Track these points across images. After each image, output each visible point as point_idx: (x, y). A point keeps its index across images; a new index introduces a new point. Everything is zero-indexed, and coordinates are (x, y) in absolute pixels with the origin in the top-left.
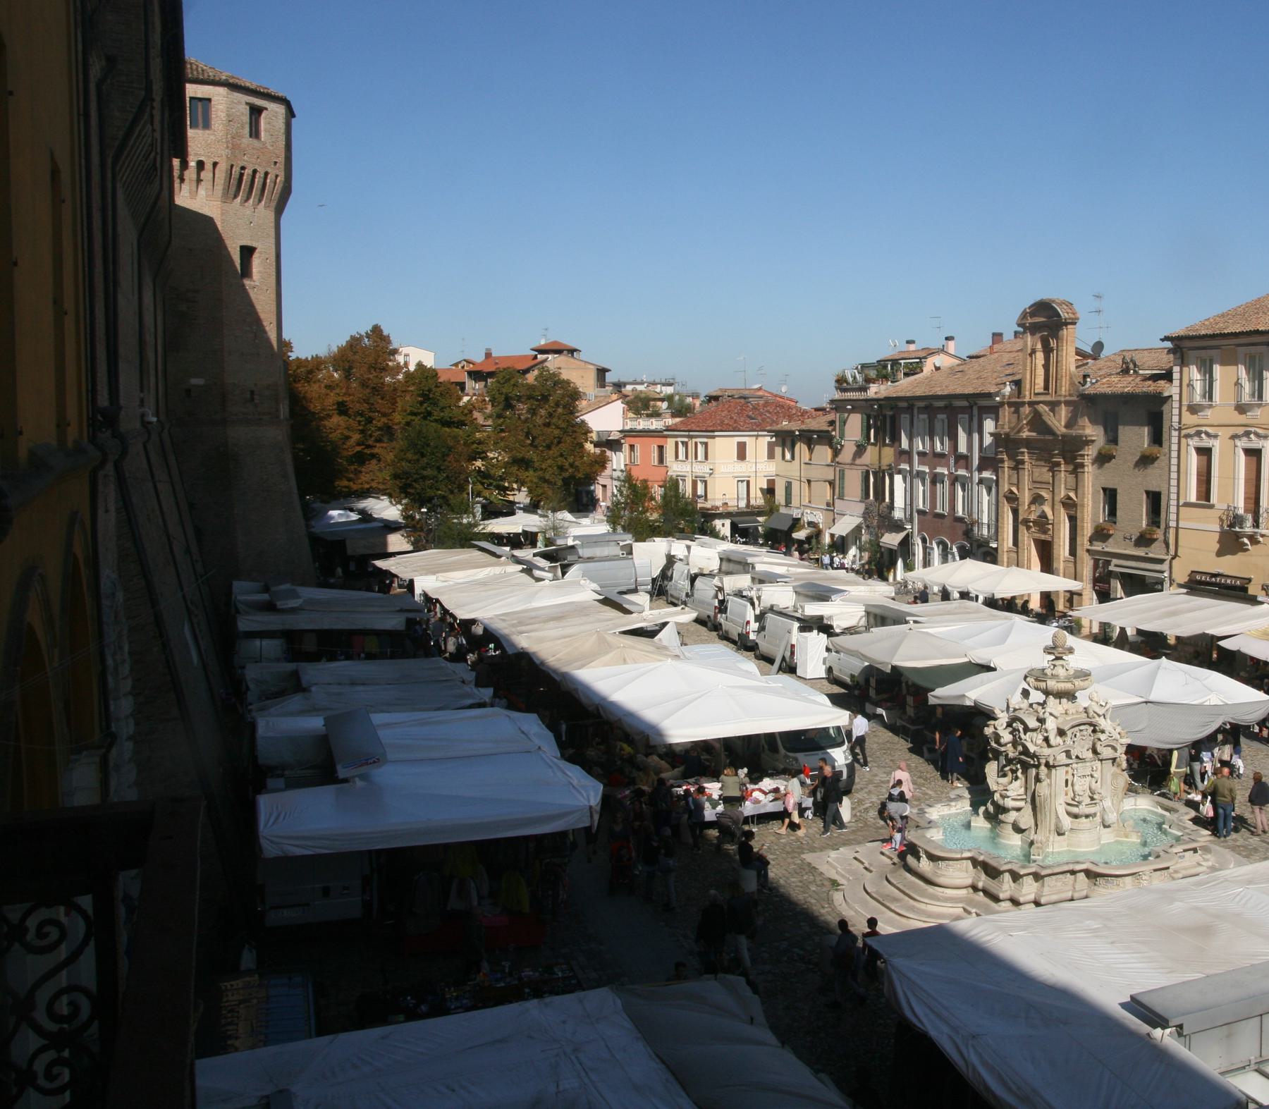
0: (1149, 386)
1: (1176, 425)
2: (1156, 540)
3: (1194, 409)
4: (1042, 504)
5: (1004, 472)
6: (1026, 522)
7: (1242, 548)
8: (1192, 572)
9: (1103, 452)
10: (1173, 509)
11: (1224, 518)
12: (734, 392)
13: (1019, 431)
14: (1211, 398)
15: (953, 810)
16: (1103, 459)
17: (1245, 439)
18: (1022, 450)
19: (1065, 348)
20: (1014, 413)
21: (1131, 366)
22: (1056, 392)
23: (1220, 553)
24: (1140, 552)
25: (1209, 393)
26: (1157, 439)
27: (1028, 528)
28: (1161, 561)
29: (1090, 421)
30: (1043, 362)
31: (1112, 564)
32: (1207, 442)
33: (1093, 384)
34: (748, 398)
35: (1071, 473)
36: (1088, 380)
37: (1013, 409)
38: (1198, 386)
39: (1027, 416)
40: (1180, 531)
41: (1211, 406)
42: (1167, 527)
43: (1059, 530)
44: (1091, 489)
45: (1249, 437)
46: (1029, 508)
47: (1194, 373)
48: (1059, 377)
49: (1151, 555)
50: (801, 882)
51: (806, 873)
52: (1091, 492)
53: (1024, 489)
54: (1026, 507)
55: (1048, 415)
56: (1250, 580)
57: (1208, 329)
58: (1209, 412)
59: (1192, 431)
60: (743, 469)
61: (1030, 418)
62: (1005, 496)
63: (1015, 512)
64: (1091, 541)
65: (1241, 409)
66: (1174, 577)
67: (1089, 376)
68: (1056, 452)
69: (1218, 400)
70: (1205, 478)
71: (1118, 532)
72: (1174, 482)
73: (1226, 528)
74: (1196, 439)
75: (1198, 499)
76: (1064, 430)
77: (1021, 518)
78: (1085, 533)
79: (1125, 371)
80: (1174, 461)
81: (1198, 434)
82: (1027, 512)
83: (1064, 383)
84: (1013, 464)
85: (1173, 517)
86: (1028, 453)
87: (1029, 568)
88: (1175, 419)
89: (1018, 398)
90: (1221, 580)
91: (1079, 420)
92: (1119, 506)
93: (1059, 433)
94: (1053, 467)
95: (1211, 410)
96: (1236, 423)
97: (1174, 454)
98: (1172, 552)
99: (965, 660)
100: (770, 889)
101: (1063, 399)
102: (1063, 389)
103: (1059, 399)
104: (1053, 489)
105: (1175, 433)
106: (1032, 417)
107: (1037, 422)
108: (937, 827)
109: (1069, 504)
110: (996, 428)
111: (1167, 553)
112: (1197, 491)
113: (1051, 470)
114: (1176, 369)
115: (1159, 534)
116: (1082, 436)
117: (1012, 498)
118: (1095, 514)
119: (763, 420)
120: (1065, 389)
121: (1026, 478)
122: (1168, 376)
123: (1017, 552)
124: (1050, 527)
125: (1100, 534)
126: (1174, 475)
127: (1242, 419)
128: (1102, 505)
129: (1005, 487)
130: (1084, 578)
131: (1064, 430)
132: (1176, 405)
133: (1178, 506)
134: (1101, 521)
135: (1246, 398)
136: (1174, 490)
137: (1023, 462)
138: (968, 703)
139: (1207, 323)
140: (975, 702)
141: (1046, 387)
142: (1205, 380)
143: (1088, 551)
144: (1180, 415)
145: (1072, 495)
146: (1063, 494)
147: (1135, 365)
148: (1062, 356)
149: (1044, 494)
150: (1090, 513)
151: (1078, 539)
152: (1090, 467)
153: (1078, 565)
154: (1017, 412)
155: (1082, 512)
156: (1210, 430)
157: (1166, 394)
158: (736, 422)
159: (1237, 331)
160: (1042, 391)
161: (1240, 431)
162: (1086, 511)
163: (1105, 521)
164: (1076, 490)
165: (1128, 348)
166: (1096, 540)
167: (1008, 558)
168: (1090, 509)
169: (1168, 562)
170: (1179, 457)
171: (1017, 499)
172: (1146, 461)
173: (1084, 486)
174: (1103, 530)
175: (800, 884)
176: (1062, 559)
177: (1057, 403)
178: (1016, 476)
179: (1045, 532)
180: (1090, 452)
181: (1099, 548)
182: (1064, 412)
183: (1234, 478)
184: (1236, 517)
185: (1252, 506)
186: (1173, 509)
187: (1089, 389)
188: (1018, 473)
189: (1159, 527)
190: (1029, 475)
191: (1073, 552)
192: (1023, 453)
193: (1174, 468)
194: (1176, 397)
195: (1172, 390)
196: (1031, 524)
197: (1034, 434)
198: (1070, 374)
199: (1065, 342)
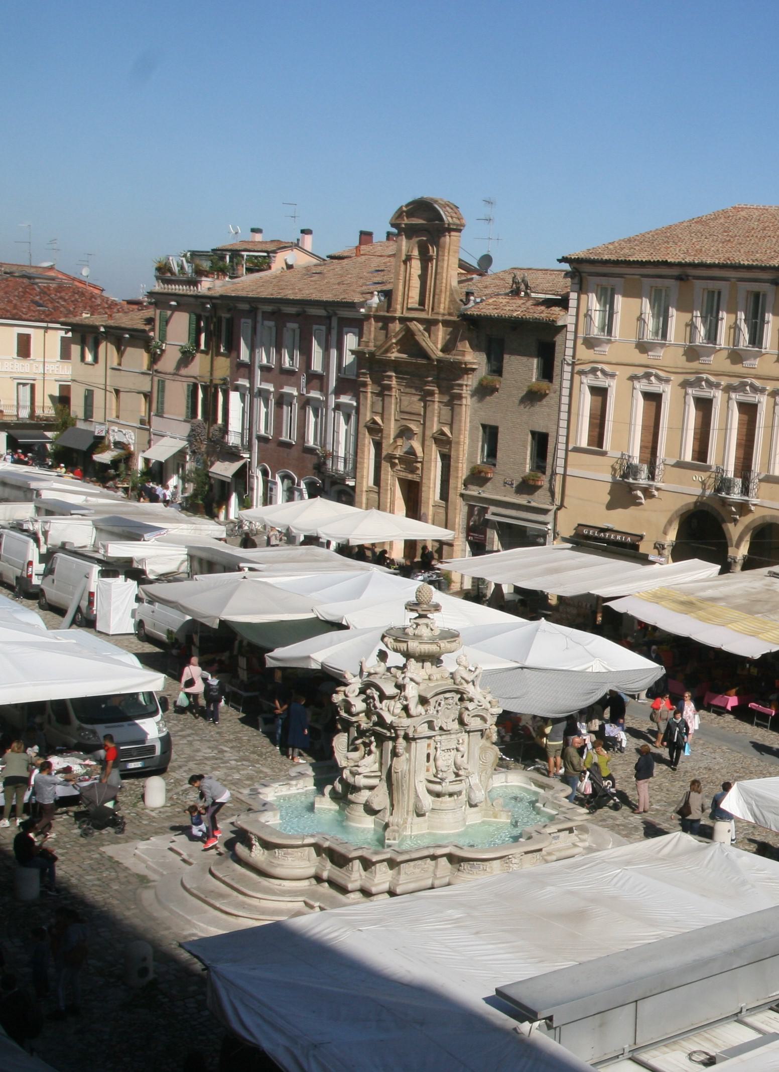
0: (542, 313)
1: (569, 359)
2: (540, 487)
3: (590, 343)
4: (410, 438)
5: (366, 398)
6: (390, 458)
7: (634, 502)
8: (579, 525)
9: (485, 383)
10: (561, 454)
11: (617, 467)
12: (14, 269)
13: (387, 351)
14: (610, 332)
15: (293, 790)
16: (484, 391)
17: (644, 381)
18: (389, 373)
19: (446, 258)
20: (381, 329)
21: (523, 287)
22: (433, 309)
23: (611, 506)
24: (522, 500)
25: (608, 326)
26: (547, 373)
27: (393, 465)
28: (545, 512)
29: (472, 347)
30: (419, 272)
31: (490, 511)
32: (602, 382)
33: (477, 303)
34: (34, 278)
35: (446, 404)
36: (472, 298)
37: (380, 324)
38: (597, 317)
39: (397, 334)
40: (568, 479)
41: (609, 342)
42: (554, 474)
43: (429, 469)
44: (468, 425)
45: (649, 380)
46: (395, 441)
47: (593, 302)
48: (438, 291)
49: (533, 504)
50: (99, 879)
51: (107, 869)
52: (468, 428)
53: (389, 420)
54: (392, 441)
55: (423, 334)
56: (641, 537)
57: (611, 254)
58: (607, 348)
59: (587, 368)
60: (25, 368)
61: (400, 336)
62: (366, 426)
63: (378, 446)
64: (466, 484)
65: (643, 347)
66: (558, 529)
67: (472, 294)
68: (430, 379)
69: (618, 335)
70: (598, 421)
71: (497, 476)
72: (563, 424)
73: (618, 478)
74: (591, 376)
75: (589, 445)
76: (440, 354)
77: (384, 453)
78: (460, 475)
79: (515, 293)
80: (565, 400)
81: (594, 371)
82: (392, 448)
83: (443, 300)
84: (377, 389)
85: (560, 462)
86: (397, 377)
87: (392, 511)
88: (569, 352)
89: (388, 312)
90: (610, 536)
91: (459, 344)
92: (499, 446)
93: (434, 357)
94: (426, 397)
95: (609, 345)
96: (637, 363)
97: (566, 392)
98: (558, 501)
99: (311, 615)
100: (58, 891)
101: (440, 318)
102: (442, 306)
103: (435, 317)
104: (424, 421)
105: (568, 369)
106: (403, 336)
107: (409, 342)
108: (273, 810)
109: (443, 442)
110: (359, 345)
111: (552, 503)
112: (589, 435)
113: (423, 399)
114: (573, 296)
115: (544, 481)
116: (461, 363)
117: (374, 429)
118: (472, 454)
119: (56, 309)
120: (443, 306)
121: (393, 407)
122: (563, 303)
123: (379, 493)
124: (419, 465)
125: (477, 477)
126: (564, 416)
127: (642, 359)
128: (480, 444)
129: (367, 416)
130: (457, 526)
131: (440, 354)
132: (570, 336)
133: (567, 450)
134: (479, 462)
135: (649, 336)
136: (563, 432)
137: (389, 388)
138: (314, 666)
139: (611, 247)
140: (322, 665)
141: (422, 302)
142: (604, 311)
143: (462, 495)
144: (575, 348)
145: (446, 430)
146: (435, 429)
147: (527, 286)
148: (442, 267)
149: (413, 427)
150: (466, 452)
151: (451, 481)
152: (469, 397)
153: (449, 511)
154: (385, 328)
155: (457, 450)
156: (607, 368)
157: (560, 323)
158: (15, 307)
159: (644, 260)
160: (416, 306)
161: (640, 372)
162: (461, 449)
163: (483, 462)
164: (451, 425)
165: (520, 267)
166: (472, 484)
167: (368, 499)
168: (466, 447)
169: (552, 513)
170: (570, 396)
171: (380, 431)
172: (533, 397)
173: (460, 421)
174: (480, 472)
175: (97, 882)
176: (431, 503)
177: (434, 322)
178: (381, 403)
179: (413, 471)
180: (470, 382)
181: (475, 493)
182: (441, 334)
183: (630, 424)
184: (630, 466)
185: (648, 456)
186: (561, 454)
187: (472, 309)
188: (383, 400)
189: (544, 473)
190: (396, 404)
191: (444, 496)
192: (390, 377)
193: (564, 408)
194: (571, 328)
195: (567, 319)
196: (397, 461)
197: (405, 356)
198: (451, 290)
199: (446, 251)
